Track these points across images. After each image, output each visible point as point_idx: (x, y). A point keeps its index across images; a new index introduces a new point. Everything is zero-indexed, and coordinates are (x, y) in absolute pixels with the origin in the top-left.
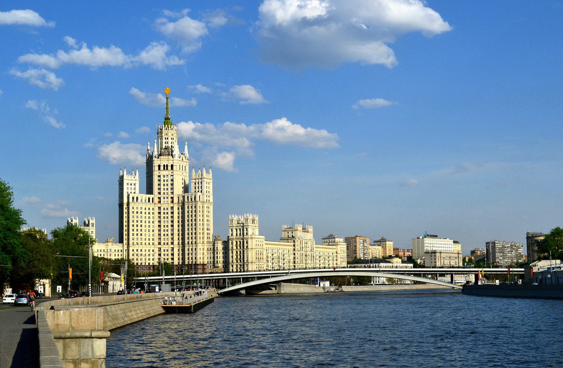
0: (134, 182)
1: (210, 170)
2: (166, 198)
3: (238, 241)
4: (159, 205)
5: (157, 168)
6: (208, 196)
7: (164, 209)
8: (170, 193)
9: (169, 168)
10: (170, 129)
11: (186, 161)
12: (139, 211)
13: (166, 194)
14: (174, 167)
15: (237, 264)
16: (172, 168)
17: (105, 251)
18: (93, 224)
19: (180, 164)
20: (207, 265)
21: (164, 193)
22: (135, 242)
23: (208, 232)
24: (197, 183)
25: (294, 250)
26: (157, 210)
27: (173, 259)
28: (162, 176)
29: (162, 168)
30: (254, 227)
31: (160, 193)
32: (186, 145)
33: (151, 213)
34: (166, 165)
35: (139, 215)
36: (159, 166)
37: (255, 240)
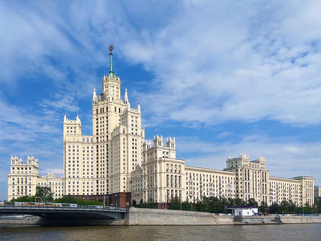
0: (75, 126)
1: (139, 105)
2: (102, 137)
5: (95, 112)
6: (134, 130)
8: (105, 132)
9: (105, 111)
10: (109, 78)
11: (125, 104)
13: (102, 133)
19: (116, 107)
24: (124, 119)
25: (237, 179)
28: (99, 119)
29: (99, 112)
30: (168, 151)
31: (97, 134)
32: (126, 91)
34: (102, 108)
36: (97, 110)
37: (166, 163)
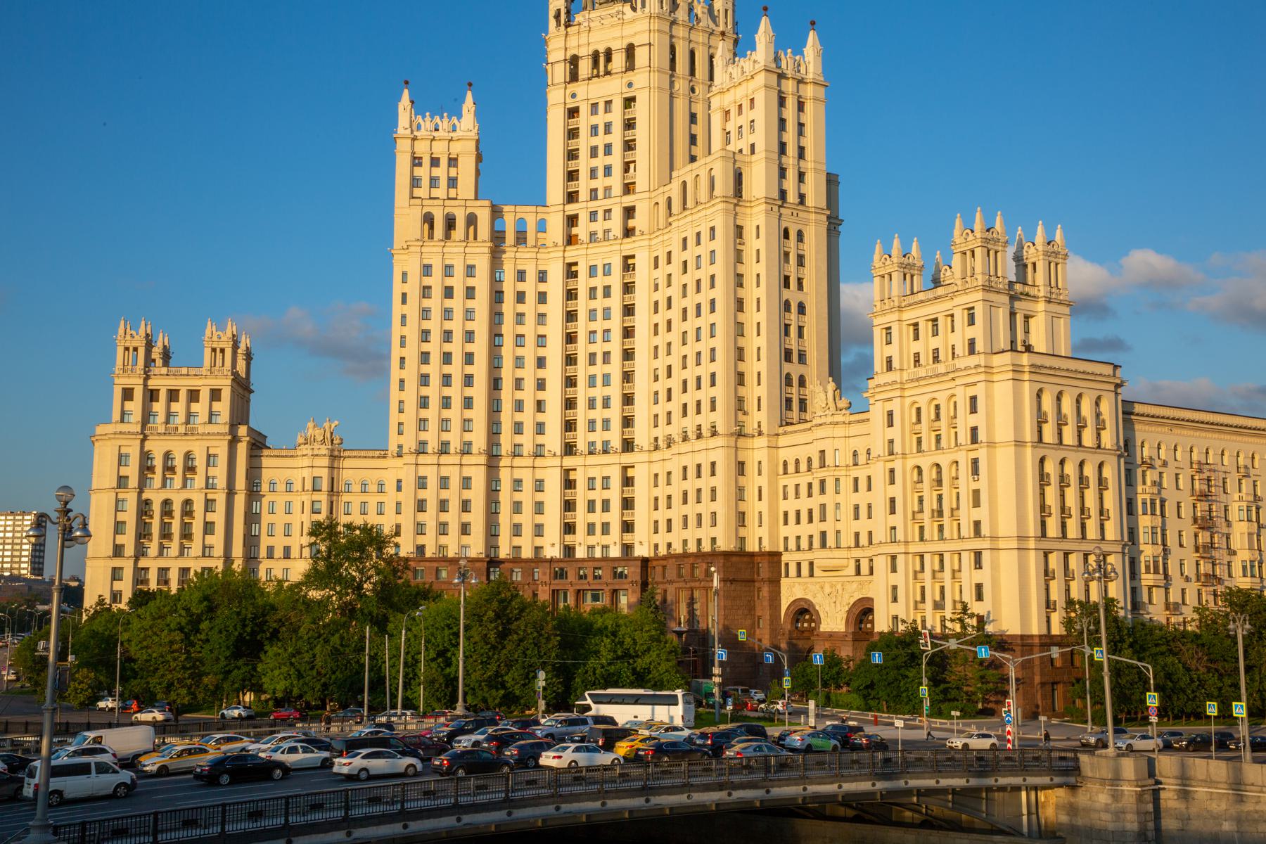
2: (600, 215)
3: (922, 402)
4: (573, 253)
5: (558, 73)
7: (592, 271)
8: (617, 189)
9: (618, 61)
12: (457, 282)
14: (641, 56)
15: (920, 548)
16: (630, 65)
17: (295, 488)
18: (222, 351)
20: (785, 558)
21: (594, 191)
22: (432, 437)
23: (794, 369)
26: (555, 287)
27: (628, 527)
28: (584, 110)
29: (585, 67)
33: (531, 298)
34: (602, 49)
35: (456, 303)
36: (574, 61)
